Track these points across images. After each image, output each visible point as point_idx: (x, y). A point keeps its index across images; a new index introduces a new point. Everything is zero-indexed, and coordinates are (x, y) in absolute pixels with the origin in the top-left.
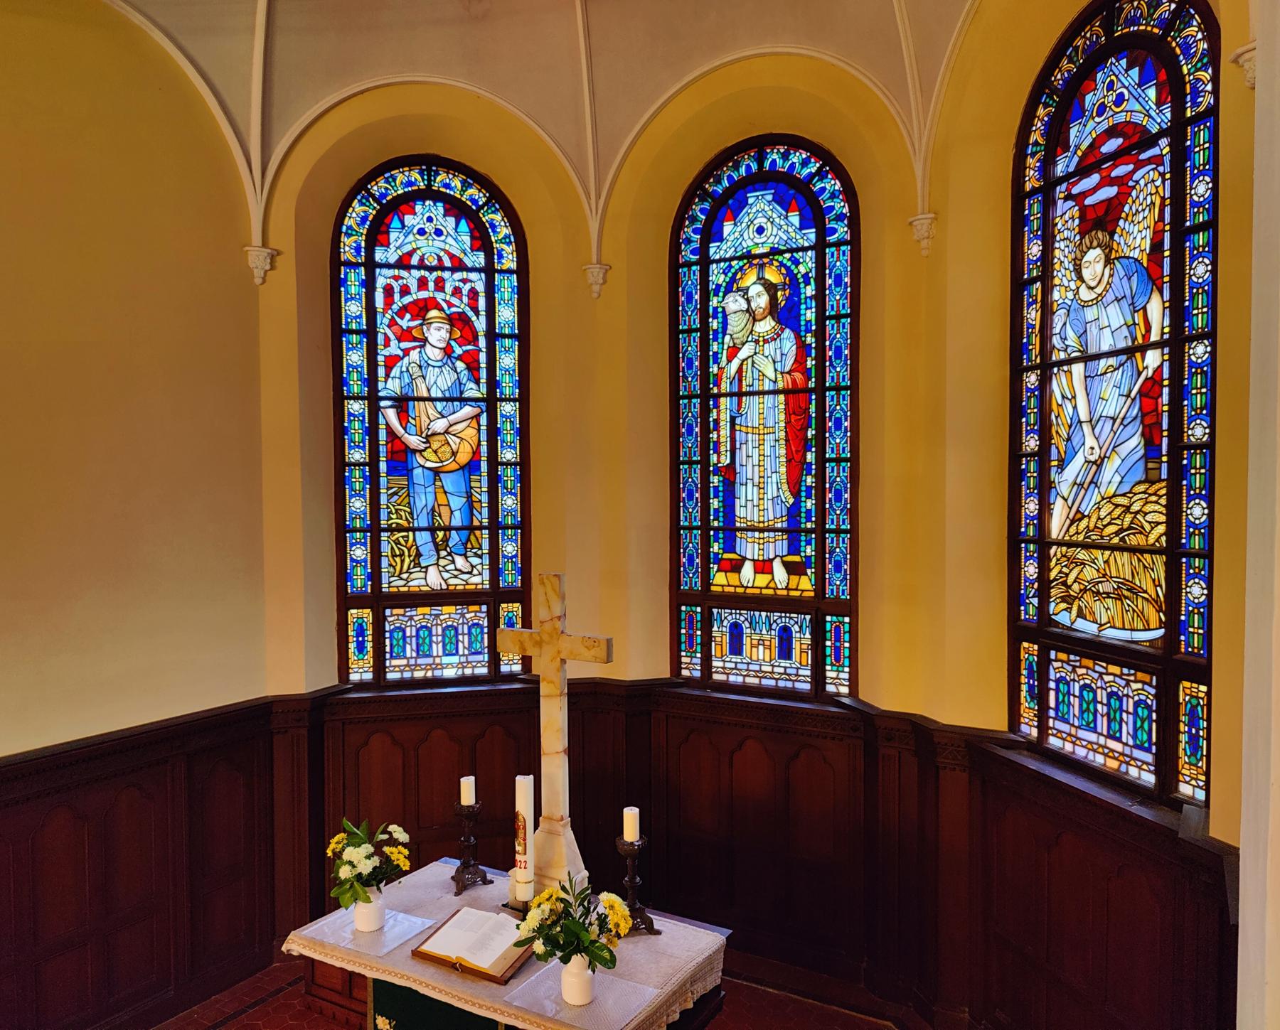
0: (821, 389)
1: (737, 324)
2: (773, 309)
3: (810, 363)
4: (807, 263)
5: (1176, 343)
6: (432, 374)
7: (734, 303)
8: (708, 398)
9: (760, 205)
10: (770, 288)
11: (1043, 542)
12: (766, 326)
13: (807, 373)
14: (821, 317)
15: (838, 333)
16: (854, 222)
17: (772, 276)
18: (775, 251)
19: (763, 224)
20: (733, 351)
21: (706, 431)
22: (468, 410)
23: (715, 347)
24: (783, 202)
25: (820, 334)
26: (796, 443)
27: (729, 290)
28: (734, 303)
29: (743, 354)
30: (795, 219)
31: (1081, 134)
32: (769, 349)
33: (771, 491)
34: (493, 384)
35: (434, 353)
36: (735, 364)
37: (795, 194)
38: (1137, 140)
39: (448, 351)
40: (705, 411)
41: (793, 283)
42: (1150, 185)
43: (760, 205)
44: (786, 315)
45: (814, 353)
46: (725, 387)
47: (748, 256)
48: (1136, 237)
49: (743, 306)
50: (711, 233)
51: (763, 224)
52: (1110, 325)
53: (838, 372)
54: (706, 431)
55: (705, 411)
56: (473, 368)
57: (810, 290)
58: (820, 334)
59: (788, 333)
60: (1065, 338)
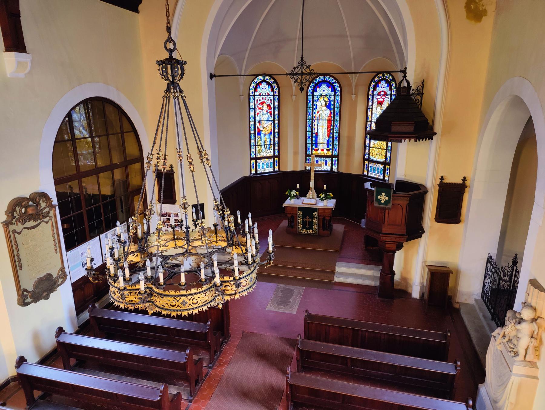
0: (334, 120)
1: (319, 107)
2: (326, 105)
3: (332, 115)
4: (332, 98)
6: (264, 116)
7: (318, 104)
10: (326, 102)
12: (325, 108)
13: (331, 117)
14: (334, 108)
17: (326, 99)
18: (326, 95)
20: (318, 112)
21: (312, 126)
22: (270, 122)
23: (314, 111)
24: (328, 86)
25: (334, 111)
27: (318, 101)
28: (318, 104)
29: (320, 113)
30: (330, 89)
32: (325, 112)
33: (324, 137)
34: (274, 117)
35: (265, 112)
36: (318, 114)
37: (330, 85)
39: (267, 111)
40: (312, 123)
41: (330, 101)
44: (328, 107)
45: (333, 114)
46: (316, 118)
47: (321, 95)
54: (312, 126)
55: (312, 123)
56: (271, 114)
57: (332, 103)
58: (334, 111)
59: (328, 110)
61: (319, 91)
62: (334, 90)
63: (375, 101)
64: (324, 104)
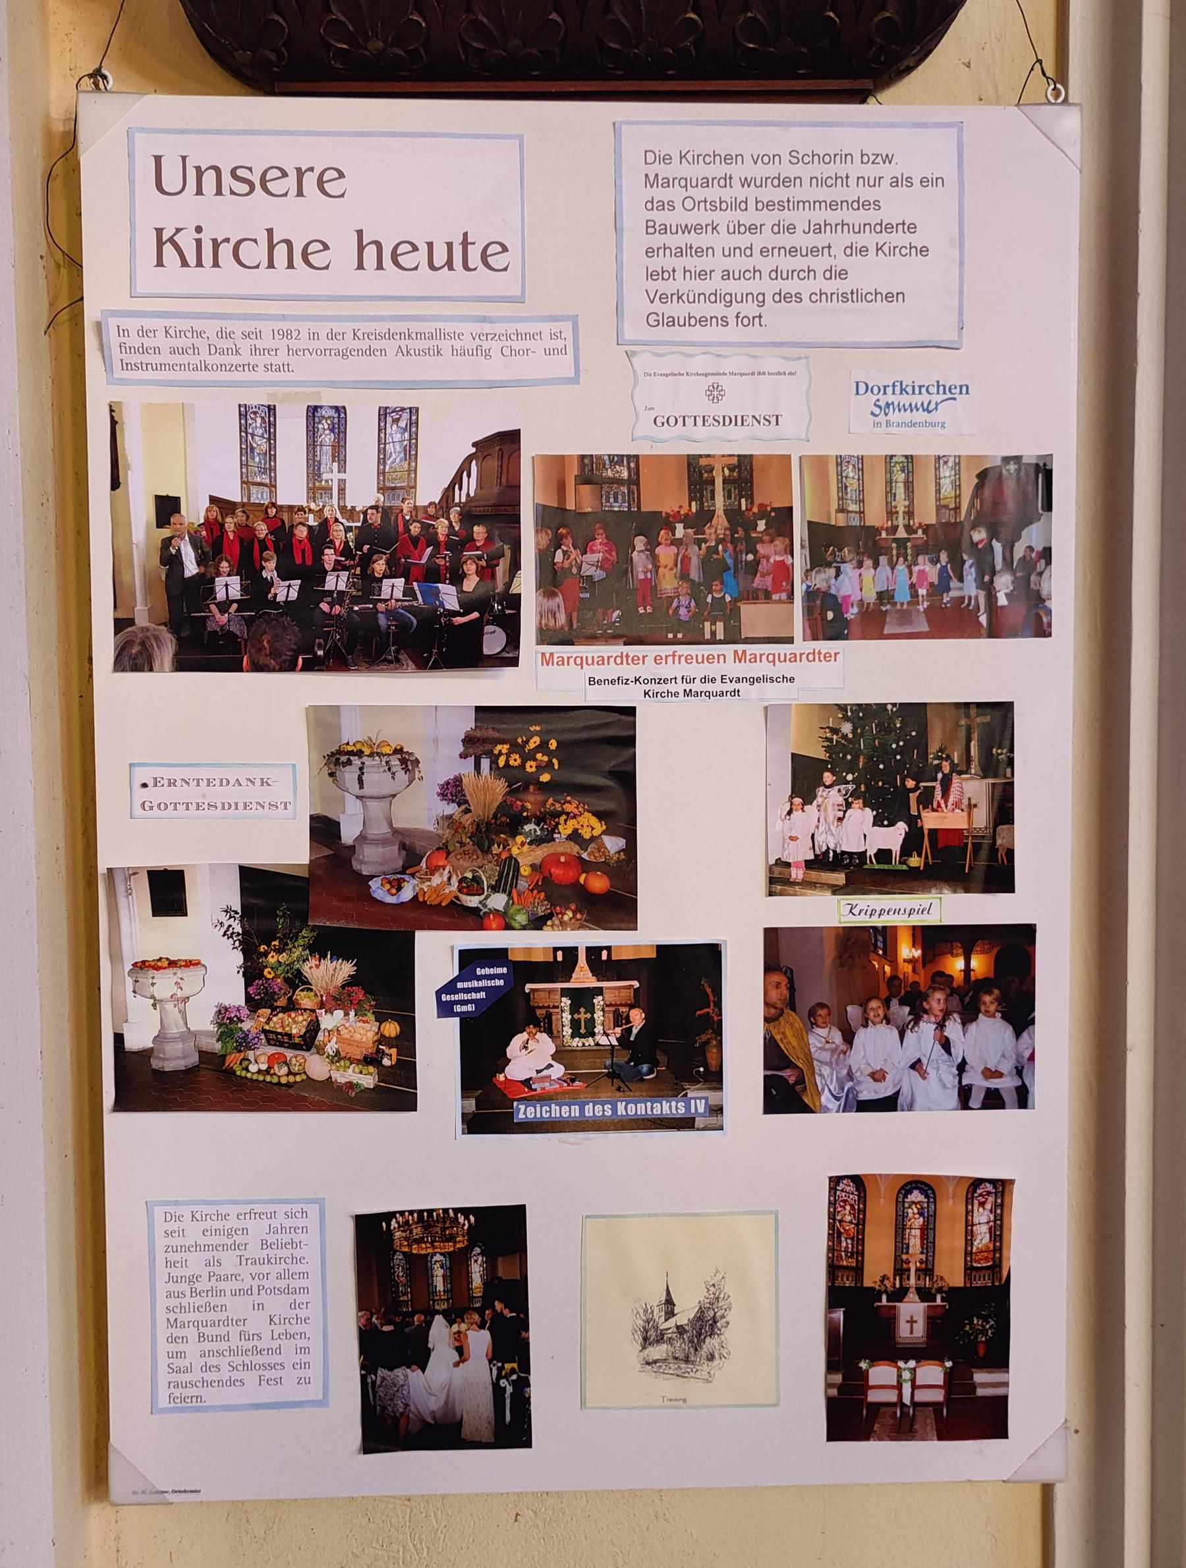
1: (910, 1215)
5: (995, 1221)
8: (904, 1229)
9: (916, 1193)
11: (971, 1252)
15: (931, 1219)
16: (935, 1198)
19: (916, 1196)
26: (922, 1239)
31: (979, 1191)
37: (923, 1192)
38: (989, 1193)
42: (991, 1199)
43: (916, 1193)
48: (988, 1206)
49: (912, 1211)
50: (905, 1196)
51: (916, 1196)
52: (984, 1219)
53: (931, 1226)
60: (976, 1220)
61: (911, 1198)
62: (927, 1196)
63: (976, 1203)
64: (916, 1211)
